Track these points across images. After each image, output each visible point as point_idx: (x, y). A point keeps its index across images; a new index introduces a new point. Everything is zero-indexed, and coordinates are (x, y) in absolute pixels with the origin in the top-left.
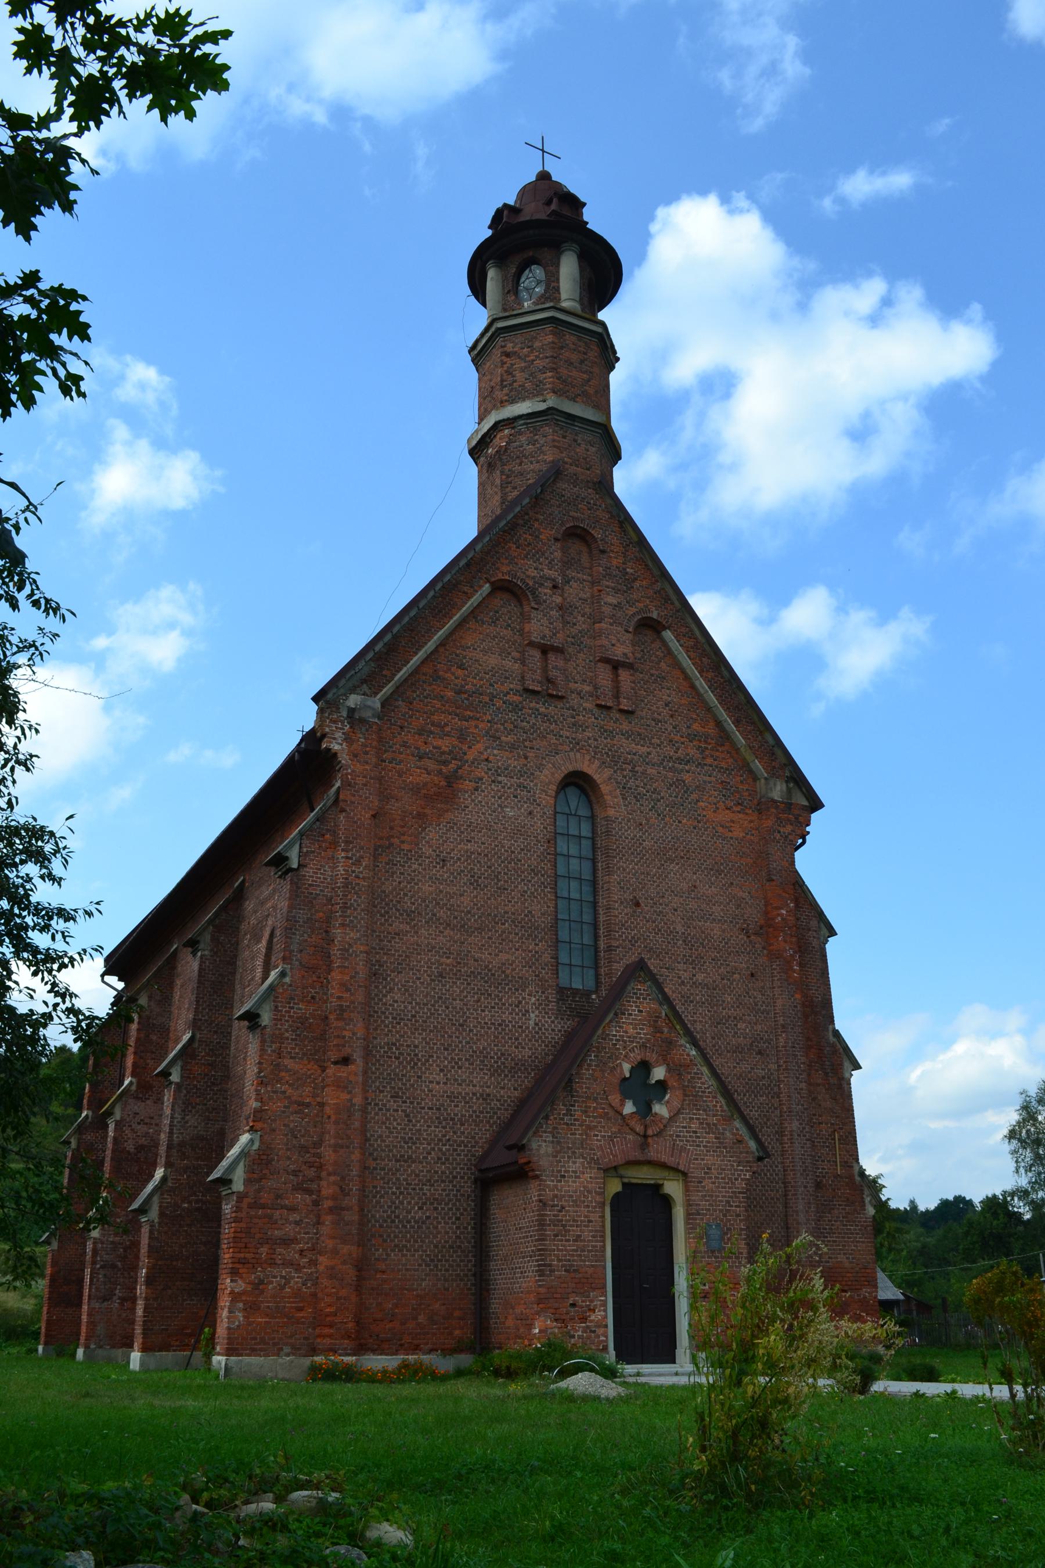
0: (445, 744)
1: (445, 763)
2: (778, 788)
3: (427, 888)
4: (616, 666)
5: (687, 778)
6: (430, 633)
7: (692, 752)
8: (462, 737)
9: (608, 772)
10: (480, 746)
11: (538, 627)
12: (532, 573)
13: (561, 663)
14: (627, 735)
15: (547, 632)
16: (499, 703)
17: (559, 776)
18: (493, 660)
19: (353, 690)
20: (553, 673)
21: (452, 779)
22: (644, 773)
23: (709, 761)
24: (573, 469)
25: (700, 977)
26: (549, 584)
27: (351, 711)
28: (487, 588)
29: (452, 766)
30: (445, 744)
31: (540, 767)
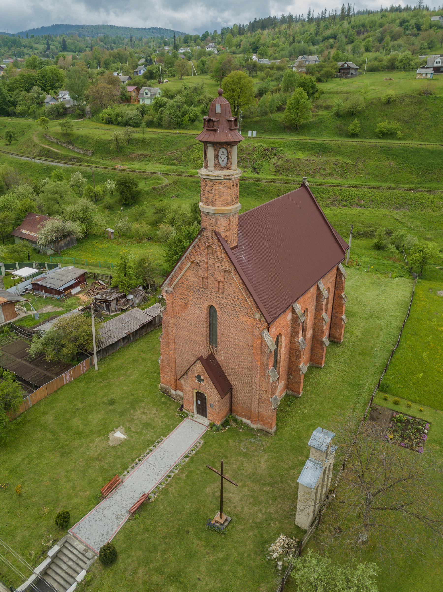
0: (185, 297)
1: (185, 301)
2: (258, 315)
3: (183, 324)
4: (219, 282)
5: (236, 309)
6: (179, 274)
7: (238, 303)
8: (188, 296)
9: (218, 306)
10: (191, 298)
11: (201, 273)
12: (199, 259)
13: (207, 281)
14: (222, 298)
15: (203, 274)
16: (195, 289)
17: (207, 306)
18: (193, 279)
19: (166, 286)
20: (204, 283)
21: (187, 304)
22: (226, 307)
23: (242, 305)
24: (209, 227)
25: (236, 352)
26: (203, 262)
27: (166, 291)
28: (190, 263)
29: (187, 301)
30: (185, 297)
31: (203, 303)
